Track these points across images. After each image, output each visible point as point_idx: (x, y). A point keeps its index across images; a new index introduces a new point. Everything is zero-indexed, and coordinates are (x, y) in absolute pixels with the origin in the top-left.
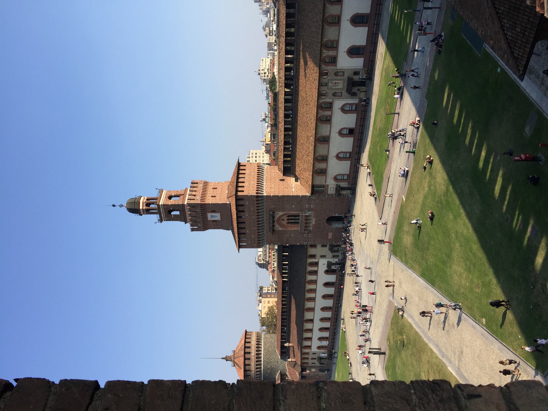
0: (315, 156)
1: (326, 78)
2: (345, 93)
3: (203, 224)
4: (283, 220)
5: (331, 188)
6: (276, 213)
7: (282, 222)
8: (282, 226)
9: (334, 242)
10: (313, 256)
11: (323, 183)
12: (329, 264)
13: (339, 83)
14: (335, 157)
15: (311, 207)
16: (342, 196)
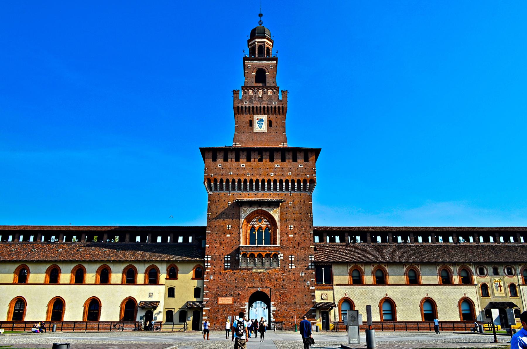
0: (385, 266)
1: (504, 272)
2: (488, 300)
3: (247, 106)
4: (260, 220)
5: (327, 294)
6: (278, 210)
7: (255, 220)
8: (249, 219)
9: (209, 308)
10: (173, 274)
11: (335, 282)
12: (155, 305)
13: (501, 291)
14: (385, 296)
15: (290, 265)
16: (313, 314)
